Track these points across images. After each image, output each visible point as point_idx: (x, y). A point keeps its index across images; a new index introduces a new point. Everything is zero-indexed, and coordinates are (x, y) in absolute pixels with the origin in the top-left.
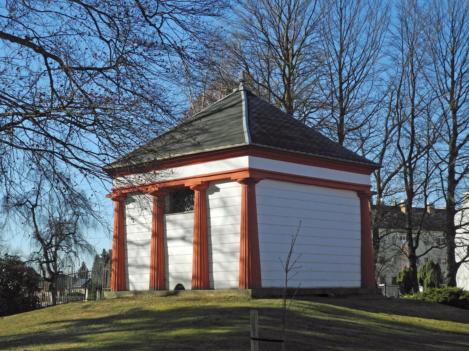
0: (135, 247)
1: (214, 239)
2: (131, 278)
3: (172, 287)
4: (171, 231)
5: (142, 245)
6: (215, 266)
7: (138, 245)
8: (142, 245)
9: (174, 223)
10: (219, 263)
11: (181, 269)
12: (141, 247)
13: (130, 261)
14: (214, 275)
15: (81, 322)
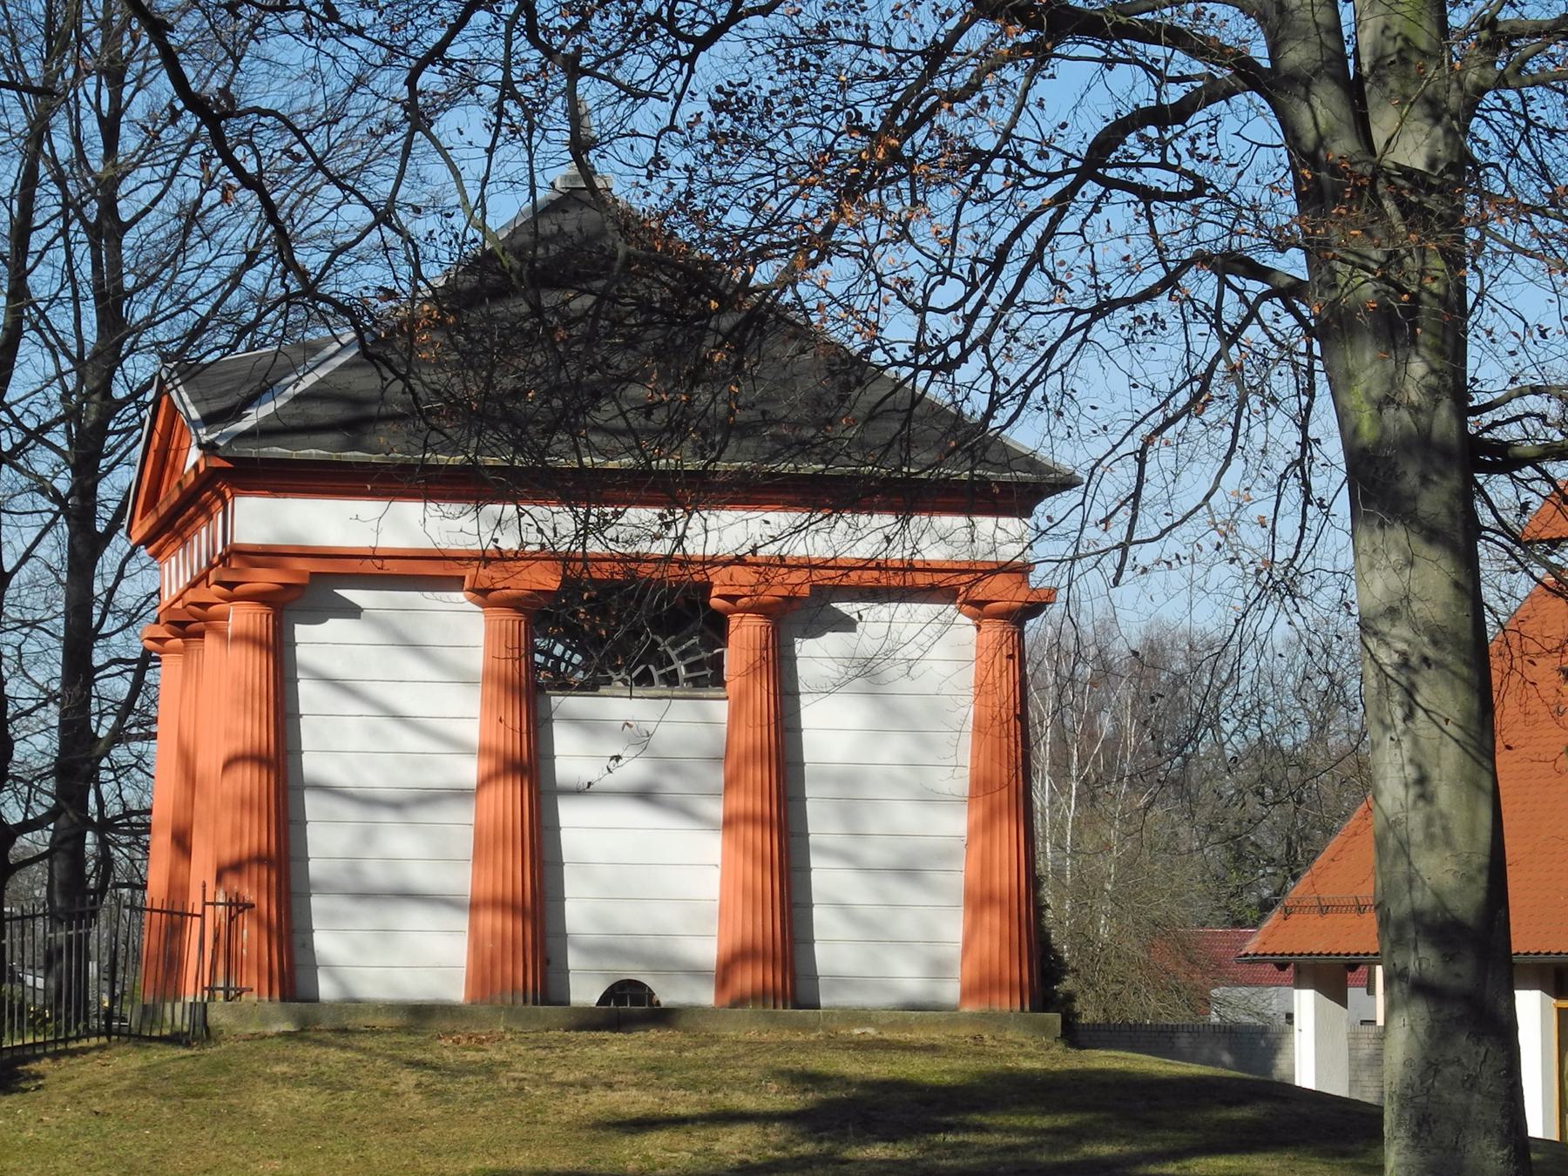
0: (349, 812)
1: (822, 823)
2: (325, 942)
3: (585, 991)
4: (572, 756)
5: (396, 805)
6: (818, 914)
7: (369, 801)
8: (396, 805)
9: (589, 726)
10: (841, 906)
11: (637, 920)
12: (386, 816)
13: (316, 868)
14: (819, 950)
15: (1050, 1138)
